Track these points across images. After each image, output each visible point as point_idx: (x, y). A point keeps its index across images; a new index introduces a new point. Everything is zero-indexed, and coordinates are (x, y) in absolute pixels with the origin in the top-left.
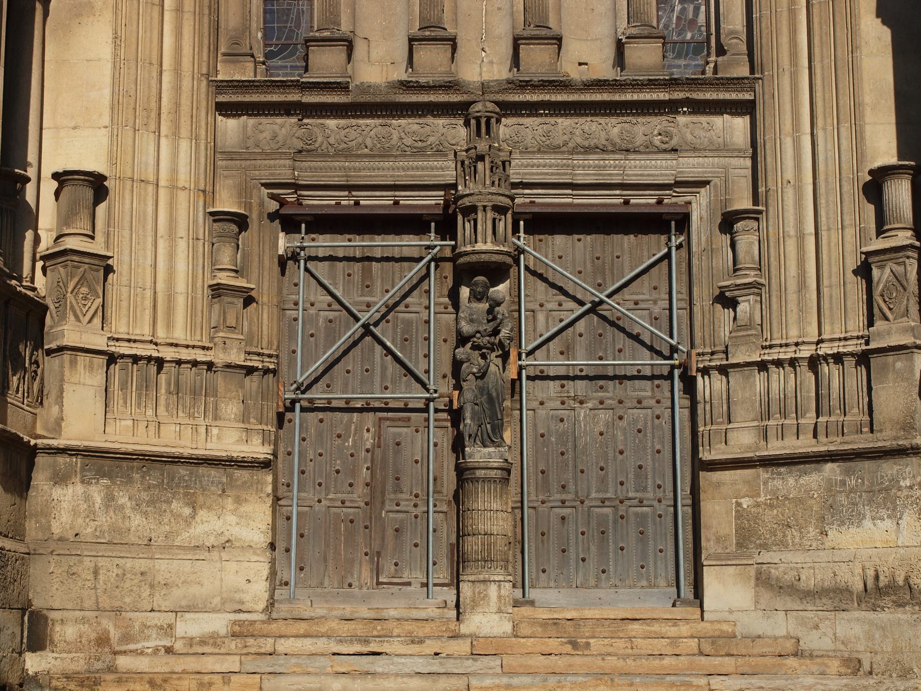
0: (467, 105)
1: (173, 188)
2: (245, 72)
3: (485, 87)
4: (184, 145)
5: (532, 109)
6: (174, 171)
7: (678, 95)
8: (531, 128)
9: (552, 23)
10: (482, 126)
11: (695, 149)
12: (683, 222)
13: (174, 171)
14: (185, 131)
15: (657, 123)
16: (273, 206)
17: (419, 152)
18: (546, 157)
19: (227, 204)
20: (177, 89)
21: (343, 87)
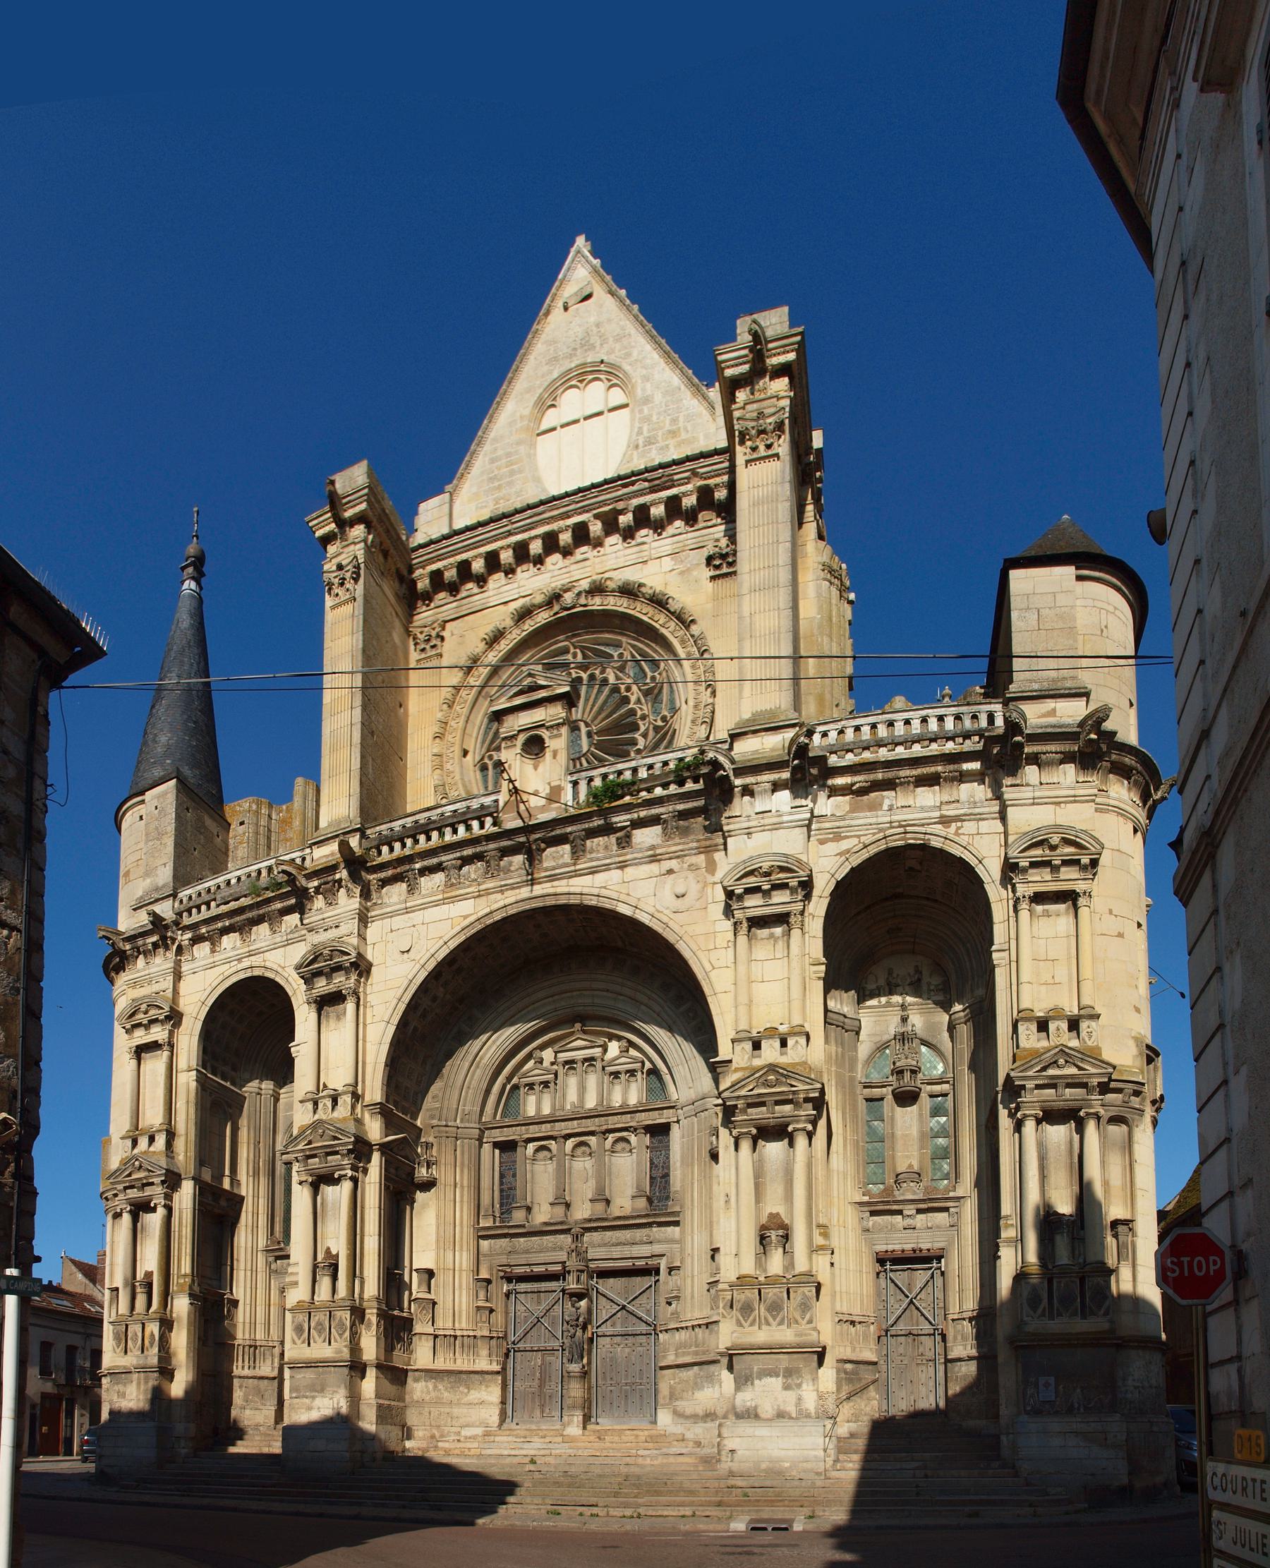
0: (570, 1230)
1: (461, 1270)
2: (489, 1223)
3: (576, 1222)
4: (465, 1254)
5: (595, 1229)
6: (461, 1263)
7: (651, 1220)
8: (595, 1237)
9: (607, 1193)
10: (577, 1238)
11: (659, 1242)
12: (657, 1272)
13: (461, 1263)
14: (465, 1248)
15: (645, 1231)
16: (502, 1274)
17: (554, 1249)
18: (601, 1249)
19: (484, 1274)
20: (462, 1232)
21: (524, 1226)
